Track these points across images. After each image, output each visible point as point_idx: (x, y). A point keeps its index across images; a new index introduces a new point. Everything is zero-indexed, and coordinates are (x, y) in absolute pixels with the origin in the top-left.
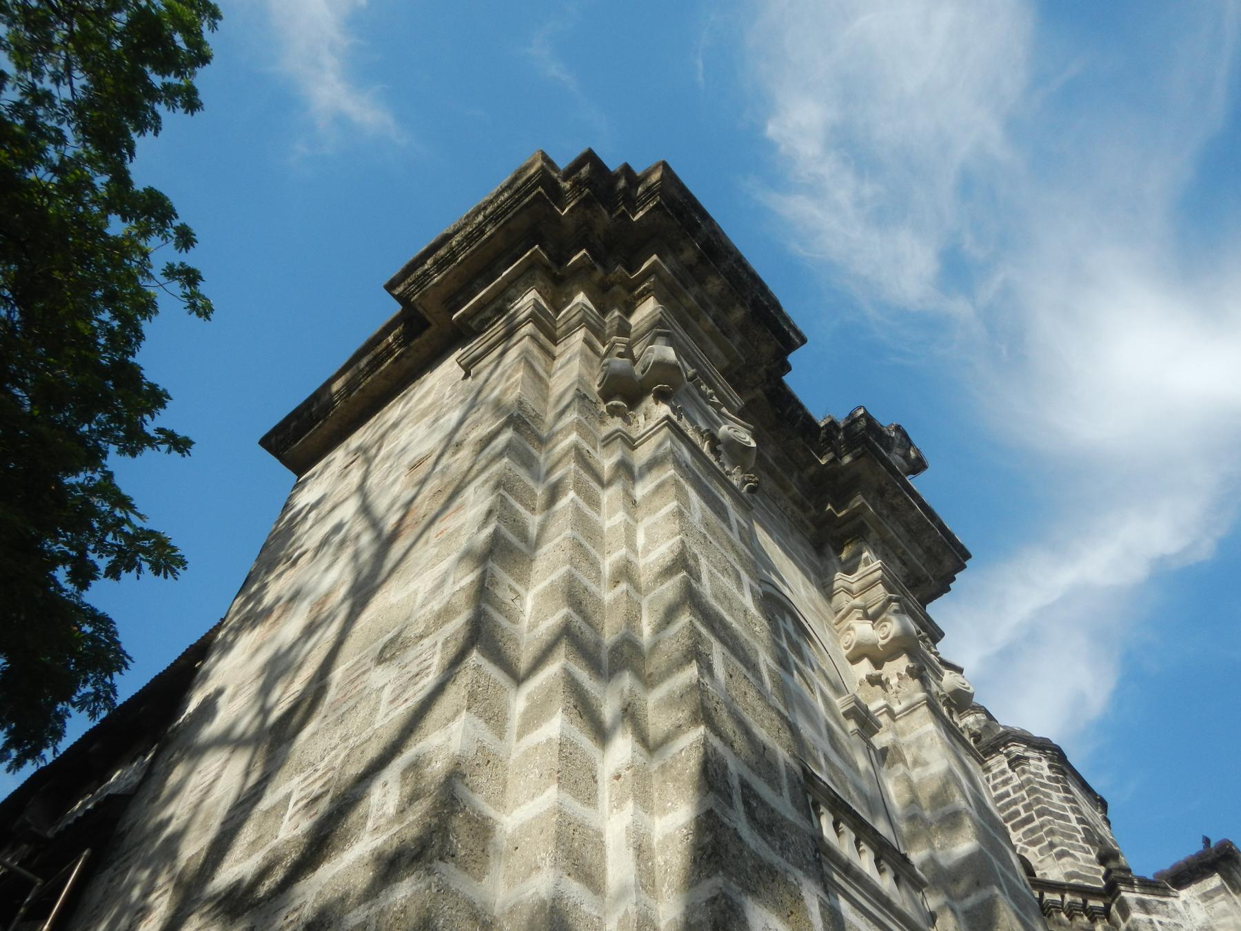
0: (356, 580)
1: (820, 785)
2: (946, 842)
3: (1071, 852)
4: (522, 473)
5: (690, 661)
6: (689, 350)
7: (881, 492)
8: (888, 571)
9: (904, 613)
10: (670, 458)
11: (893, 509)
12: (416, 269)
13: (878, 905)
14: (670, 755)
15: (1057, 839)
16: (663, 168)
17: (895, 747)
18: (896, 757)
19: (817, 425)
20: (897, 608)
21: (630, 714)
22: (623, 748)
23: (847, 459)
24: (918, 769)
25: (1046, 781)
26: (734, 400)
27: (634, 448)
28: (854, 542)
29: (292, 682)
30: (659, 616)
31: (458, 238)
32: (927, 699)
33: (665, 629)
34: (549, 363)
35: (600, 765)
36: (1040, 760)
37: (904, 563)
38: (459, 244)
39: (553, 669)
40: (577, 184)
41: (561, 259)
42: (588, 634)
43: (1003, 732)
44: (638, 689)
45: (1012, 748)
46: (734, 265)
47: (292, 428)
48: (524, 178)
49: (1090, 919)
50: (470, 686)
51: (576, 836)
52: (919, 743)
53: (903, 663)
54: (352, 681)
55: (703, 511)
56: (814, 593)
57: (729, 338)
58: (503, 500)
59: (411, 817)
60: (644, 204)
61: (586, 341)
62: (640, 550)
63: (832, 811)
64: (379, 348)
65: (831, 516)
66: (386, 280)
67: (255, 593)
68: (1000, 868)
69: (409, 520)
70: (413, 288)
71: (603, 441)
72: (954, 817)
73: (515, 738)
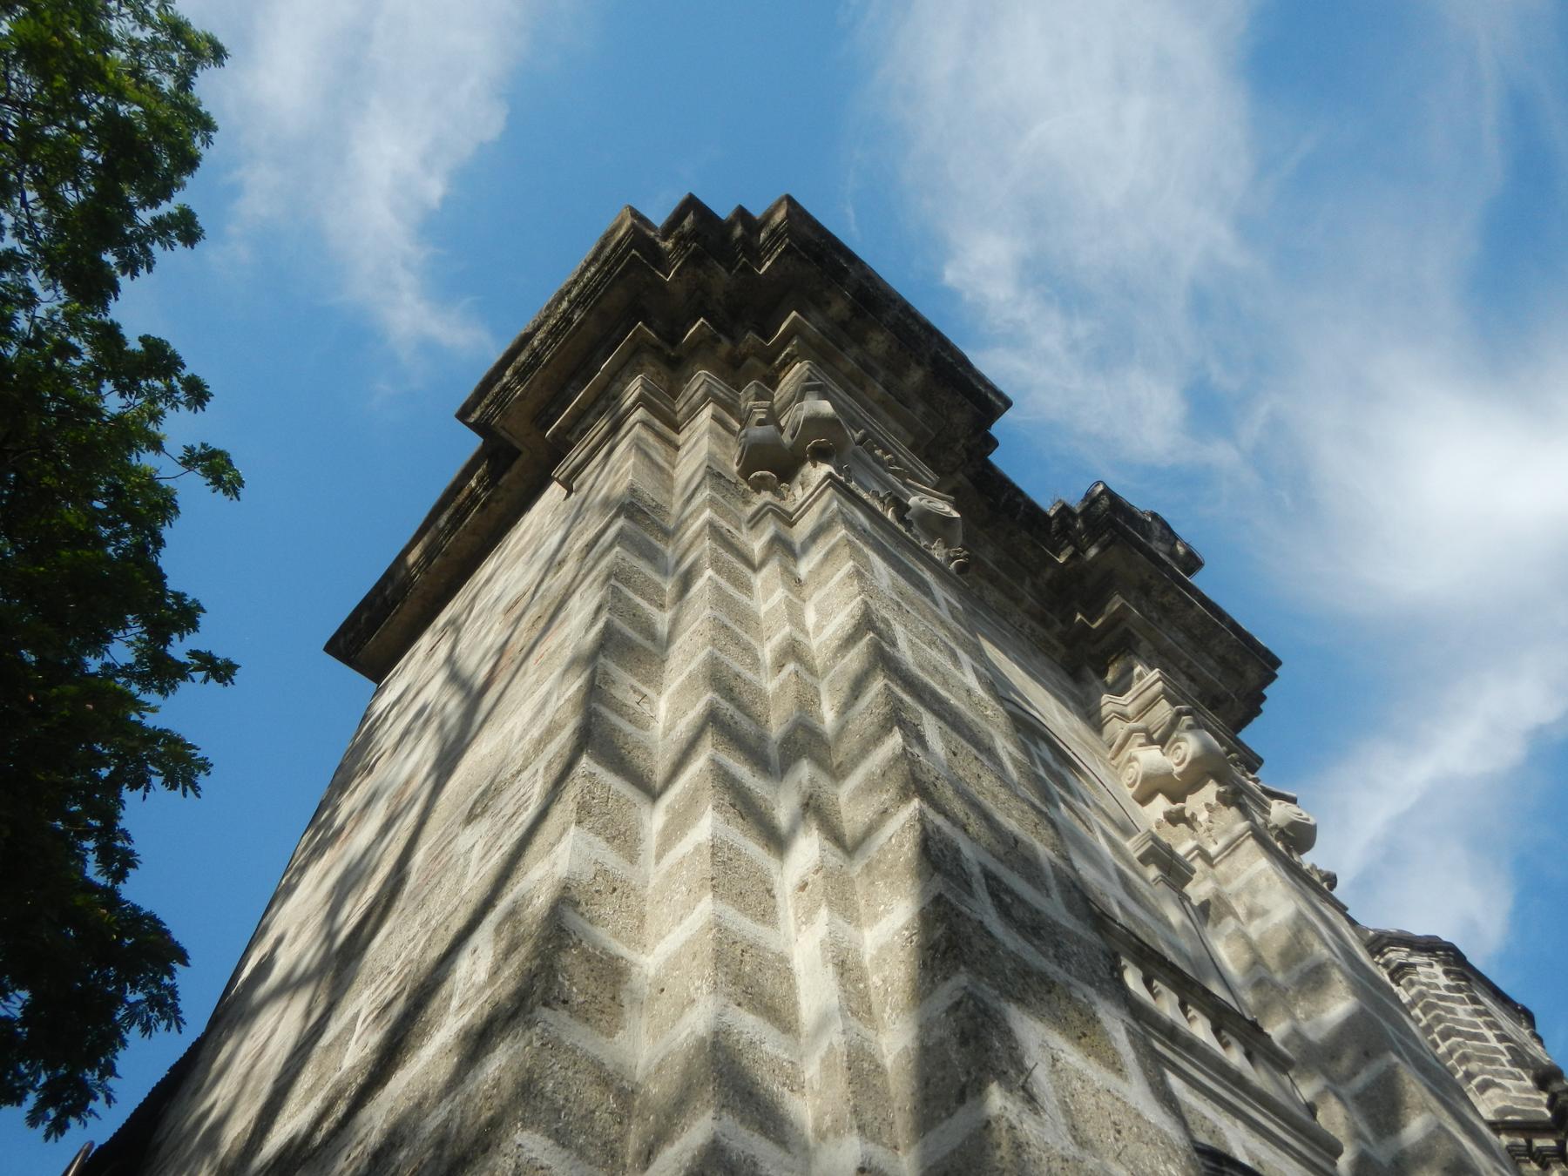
0: (442, 750)
1: (1114, 929)
2: (1313, 1008)
3: (1497, 1080)
4: (642, 565)
5: (891, 730)
6: (854, 414)
7: (1145, 590)
8: (1169, 680)
9: (1200, 728)
10: (839, 519)
11: (1165, 610)
12: (492, 386)
13: (1226, 1083)
14: (876, 849)
15: (1474, 1066)
16: (789, 204)
17: (1218, 897)
18: (1223, 909)
19: (1045, 515)
20: (1191, 722)
21: (814, 809)
22: (808, 848)
23: (1093, 552)
24: (1257, 922)
25: (1444, 992)
26: (924, 474)
27: (792, 525)
28: (1121, 657)
29: (365, 890)
30: (840, 697)
31: (540, 335)
32: (1251, 829)
33: (853, 705)
34: (671, 453)
35: (777, 879)
36: (1431, 965)
37: (1192, 679)
38: (542, 342)
39: (699, 764)
40: (682, 240)
41: (673, 337)
42: (745, 725)
43: (1373, 937)
44: (823, 780)
45: (1391, 955)
46: (900, 315)
47: (363, 621)
48: (613, 244)
49: (1540, 1165)
50: (579, 797)
51: (747, 957)
52: (1251, 887)
53: (1211, 790)
54: (437, 857)
55: (892, 579)
56: (1076, 722)
57: (908, 407)
58: (615, 590)
59: (507, 972)
60: (770, 251)
61: (714, 417)
62: (811, 630)
63: (1139, 965)
64: (461, 498)
65: (1084, 628)
66: (457, 408)
67: (326, 819)
68: (1395, 1034)
69: (504, 662)
70: (491, 410)
71: (749, 522)
72: (1317, 973)
73: (653, 861)
